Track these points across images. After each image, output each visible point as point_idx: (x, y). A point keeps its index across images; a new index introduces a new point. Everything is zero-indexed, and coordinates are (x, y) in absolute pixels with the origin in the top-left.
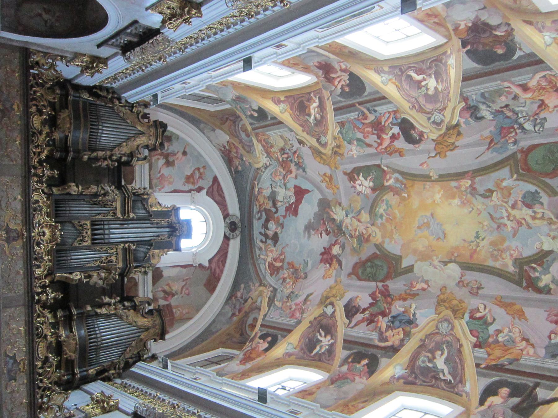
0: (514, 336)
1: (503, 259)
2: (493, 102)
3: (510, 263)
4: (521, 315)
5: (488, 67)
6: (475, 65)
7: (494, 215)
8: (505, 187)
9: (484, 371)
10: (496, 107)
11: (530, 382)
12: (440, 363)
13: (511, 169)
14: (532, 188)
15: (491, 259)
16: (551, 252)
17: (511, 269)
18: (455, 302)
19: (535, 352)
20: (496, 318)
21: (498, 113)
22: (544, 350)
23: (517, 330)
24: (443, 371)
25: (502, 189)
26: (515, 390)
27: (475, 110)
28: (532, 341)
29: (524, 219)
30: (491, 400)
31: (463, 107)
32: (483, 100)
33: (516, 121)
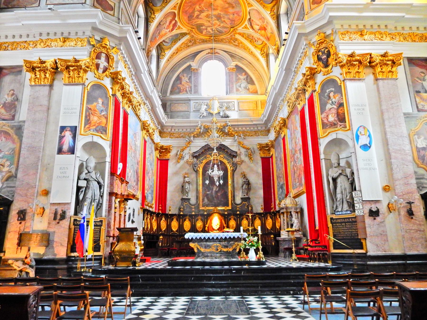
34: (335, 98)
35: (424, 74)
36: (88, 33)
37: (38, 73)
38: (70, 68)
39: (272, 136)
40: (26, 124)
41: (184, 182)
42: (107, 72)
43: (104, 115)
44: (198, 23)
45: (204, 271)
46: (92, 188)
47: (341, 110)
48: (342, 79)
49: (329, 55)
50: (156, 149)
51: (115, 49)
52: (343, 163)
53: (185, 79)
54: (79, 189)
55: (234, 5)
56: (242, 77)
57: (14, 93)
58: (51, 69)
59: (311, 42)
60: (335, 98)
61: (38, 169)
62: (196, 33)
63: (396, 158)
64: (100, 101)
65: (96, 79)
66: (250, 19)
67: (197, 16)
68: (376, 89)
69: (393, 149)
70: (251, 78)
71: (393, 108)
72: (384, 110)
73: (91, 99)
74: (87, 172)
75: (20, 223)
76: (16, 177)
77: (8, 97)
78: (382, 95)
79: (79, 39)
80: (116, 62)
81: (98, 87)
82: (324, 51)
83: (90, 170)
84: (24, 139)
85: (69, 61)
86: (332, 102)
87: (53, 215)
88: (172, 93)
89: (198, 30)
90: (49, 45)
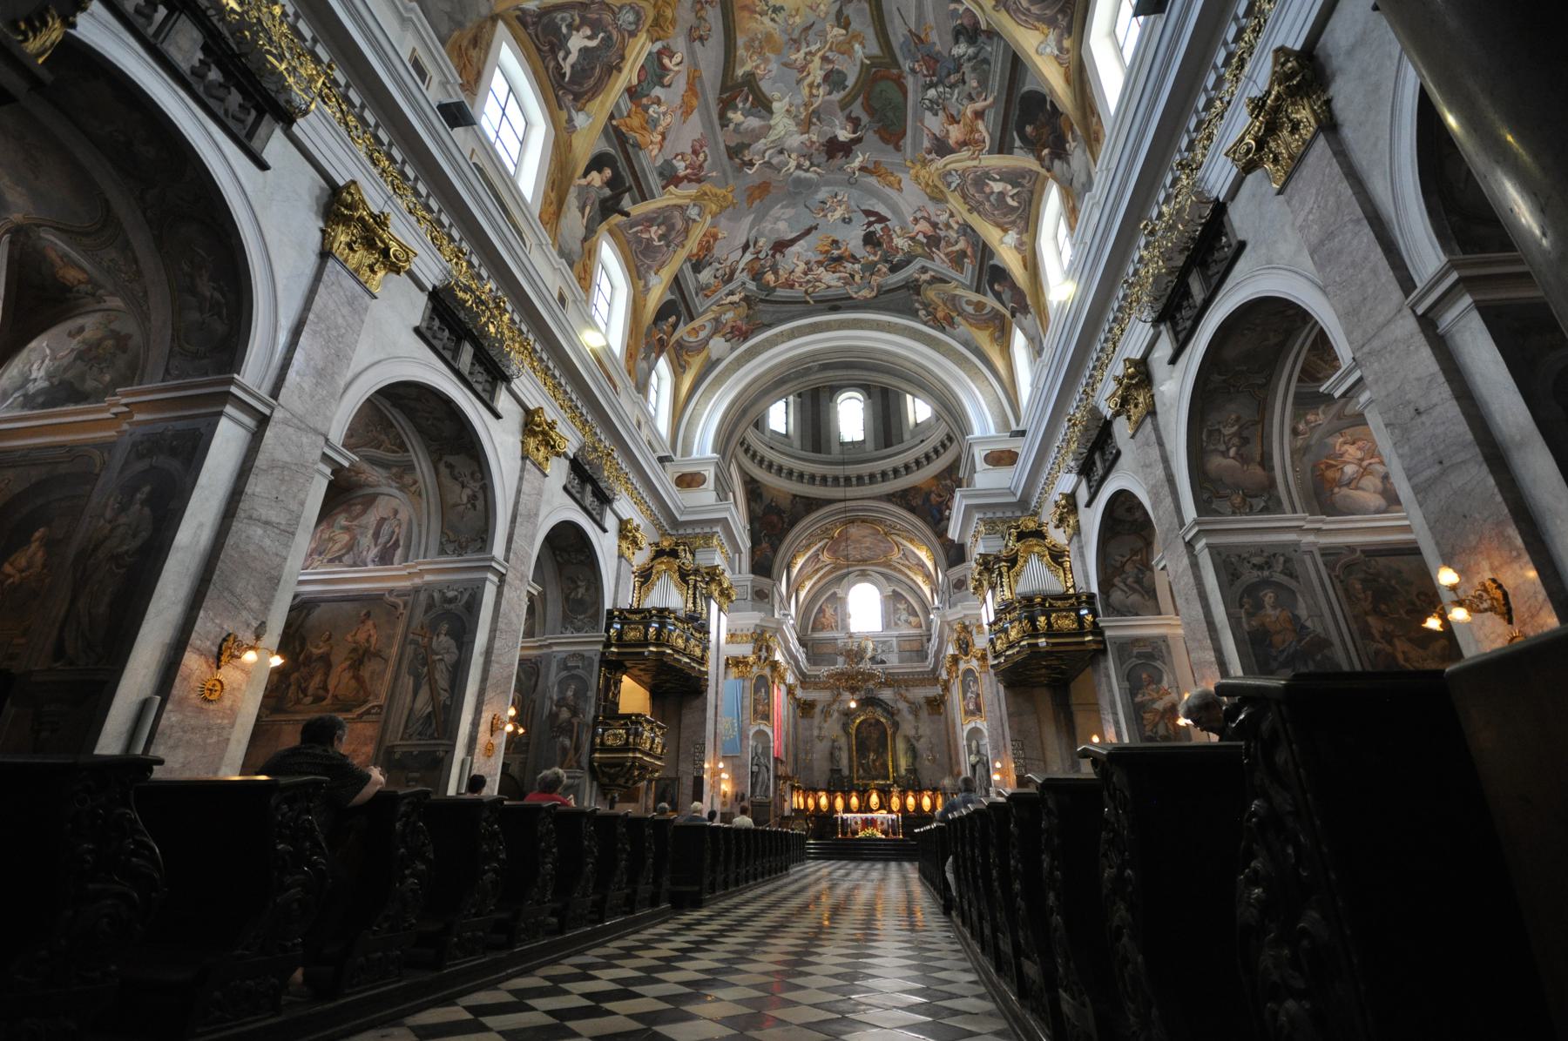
0: (662, 122)
1: (751, 57)
2: (974, 69)
3: (748, 67)
4: (687, 112)
5: (1018, 100)
6: (1026, 88)
7: (810, 32)
8: (852, 47)
9: (611, 129)
10: (967, 68)
11: (629, 181)
12: (577, 42)
13: (877, 57)
14: (850, 82)
15: (746, 39)
16: (770, 112)
17: (740, 72)
18: (669, 13)
19: (656, 156)
20: (673, 86)
21: (957, 64)
22: (662, 161)
23: (669, 120)
24: (568, 53)
25: (849, 43)
26: (615, 183)
27: (971, 38)
28: (666, 143)
29: (809, 74)
30: (594, 174)
31: (979, 22)
32: (981, 57)
33: (941, 82)
36: (752, 631)
39: (938, 690)
41: (833, 748)
49: (967, 645)
50: (798, 706)
52: (983, 752)
53: (829, 611)
54: (752, 773)
56: (902, 606)
64: (763, 690)
66: (904, 554)
70: (913, 608)
73: (757, 690)
81: (761, 678)
85: (737, 657)
88: (813, 630)
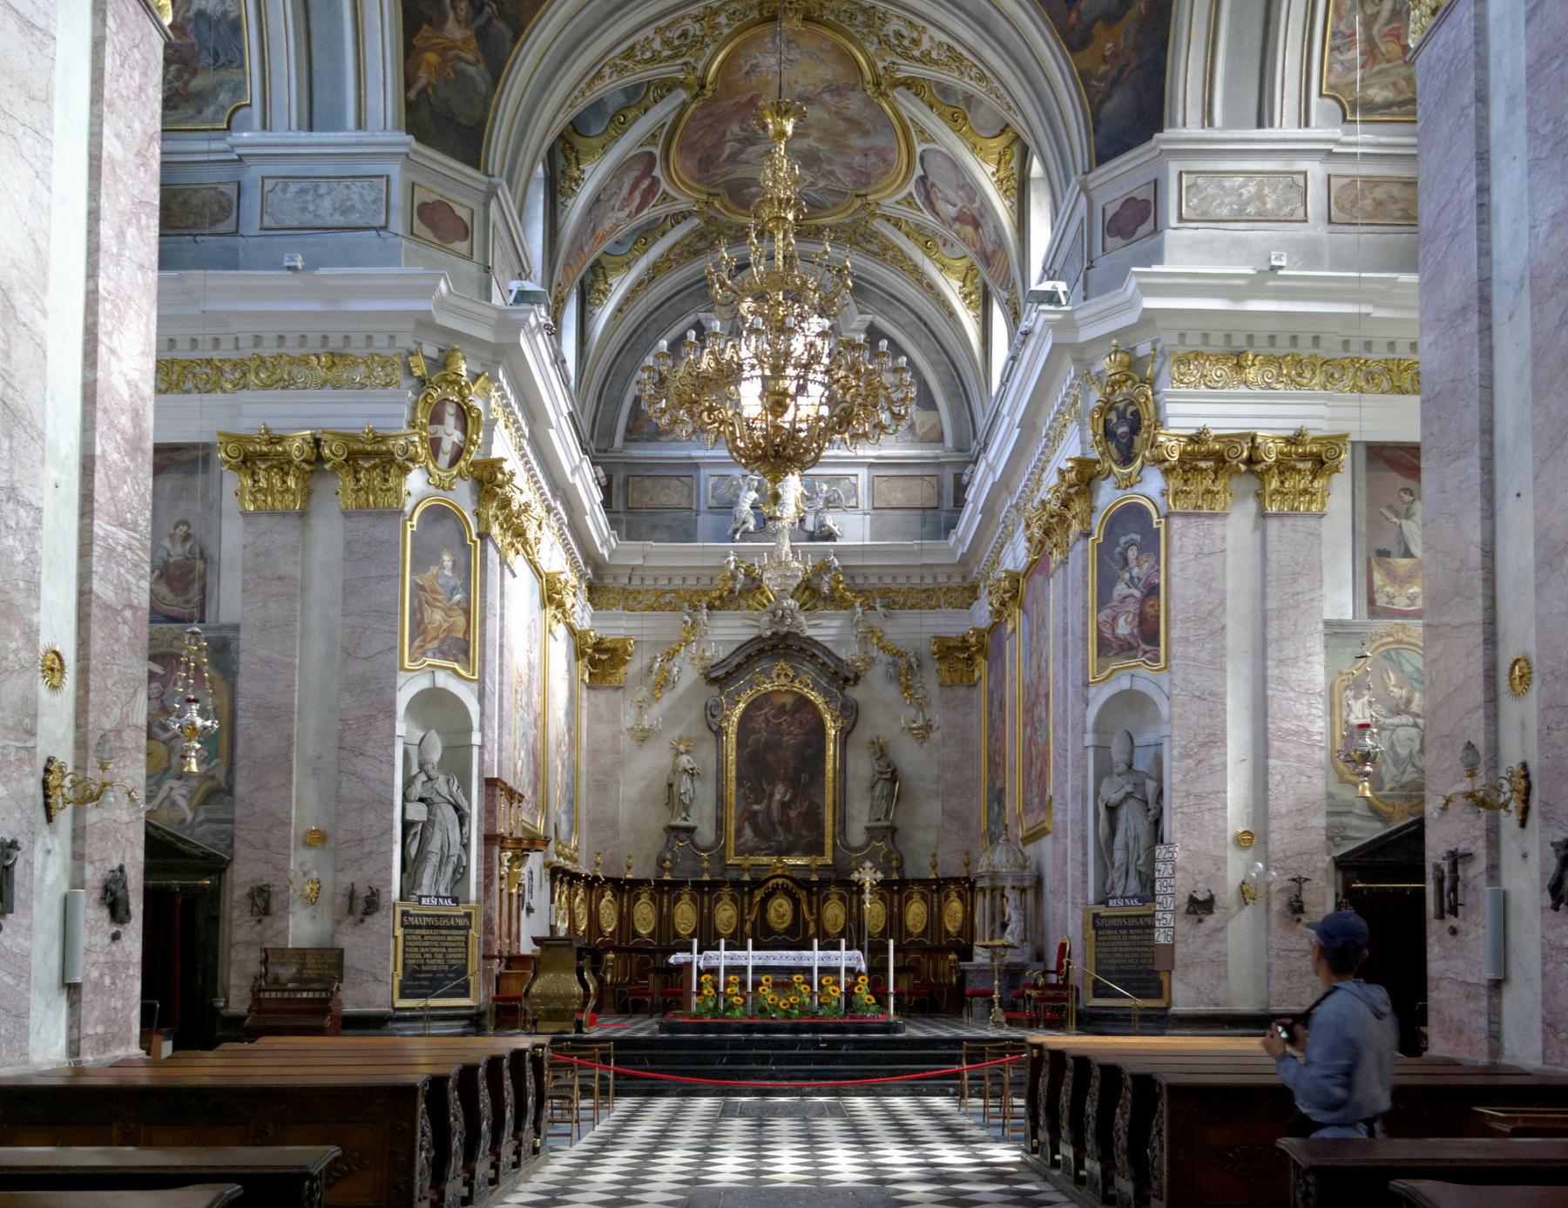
34: (1139, 569)
35: (1412, 495)
37: (261, 475)
38: (361, 462)
40: (244, 635)
42: (462, 463)
43: (459, 603)
44: (737, 175)
45: (749, 1044)
46: (440, 823)
47: (1152, 606)
48: (1164, 511)
49: (1135, 427)
51: (482, 379)
54: (407, 826)
55: (869, 126)
57: (191, 531)
58: (304, 466)
59: (1093, 372)
60: (1139, 566)
61: (290, 772)
62: (726, 208)
63: (1282, 755)
64: (447, 559)
65: (432, 490)
67: (730, 156)
68: (1258, 545)
69: (1279, 729)
71: (1296, 607)
72: (1269, 613)
74: (425, 779)
75: (260, 921)
76: (230, 791)
77: (174, 545)
78: (1273, 567)
79: (376, 358)
80: (486, 425)
82: (1125, 409)
83: (433, 773)
84: (243, 684)
86: (1132, 578)
87: (346, 900)
89: (732, 196)
90: (286, 377)
